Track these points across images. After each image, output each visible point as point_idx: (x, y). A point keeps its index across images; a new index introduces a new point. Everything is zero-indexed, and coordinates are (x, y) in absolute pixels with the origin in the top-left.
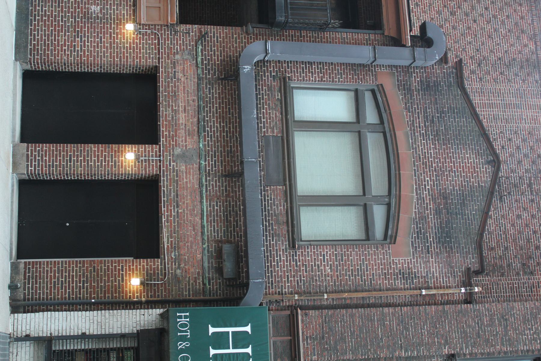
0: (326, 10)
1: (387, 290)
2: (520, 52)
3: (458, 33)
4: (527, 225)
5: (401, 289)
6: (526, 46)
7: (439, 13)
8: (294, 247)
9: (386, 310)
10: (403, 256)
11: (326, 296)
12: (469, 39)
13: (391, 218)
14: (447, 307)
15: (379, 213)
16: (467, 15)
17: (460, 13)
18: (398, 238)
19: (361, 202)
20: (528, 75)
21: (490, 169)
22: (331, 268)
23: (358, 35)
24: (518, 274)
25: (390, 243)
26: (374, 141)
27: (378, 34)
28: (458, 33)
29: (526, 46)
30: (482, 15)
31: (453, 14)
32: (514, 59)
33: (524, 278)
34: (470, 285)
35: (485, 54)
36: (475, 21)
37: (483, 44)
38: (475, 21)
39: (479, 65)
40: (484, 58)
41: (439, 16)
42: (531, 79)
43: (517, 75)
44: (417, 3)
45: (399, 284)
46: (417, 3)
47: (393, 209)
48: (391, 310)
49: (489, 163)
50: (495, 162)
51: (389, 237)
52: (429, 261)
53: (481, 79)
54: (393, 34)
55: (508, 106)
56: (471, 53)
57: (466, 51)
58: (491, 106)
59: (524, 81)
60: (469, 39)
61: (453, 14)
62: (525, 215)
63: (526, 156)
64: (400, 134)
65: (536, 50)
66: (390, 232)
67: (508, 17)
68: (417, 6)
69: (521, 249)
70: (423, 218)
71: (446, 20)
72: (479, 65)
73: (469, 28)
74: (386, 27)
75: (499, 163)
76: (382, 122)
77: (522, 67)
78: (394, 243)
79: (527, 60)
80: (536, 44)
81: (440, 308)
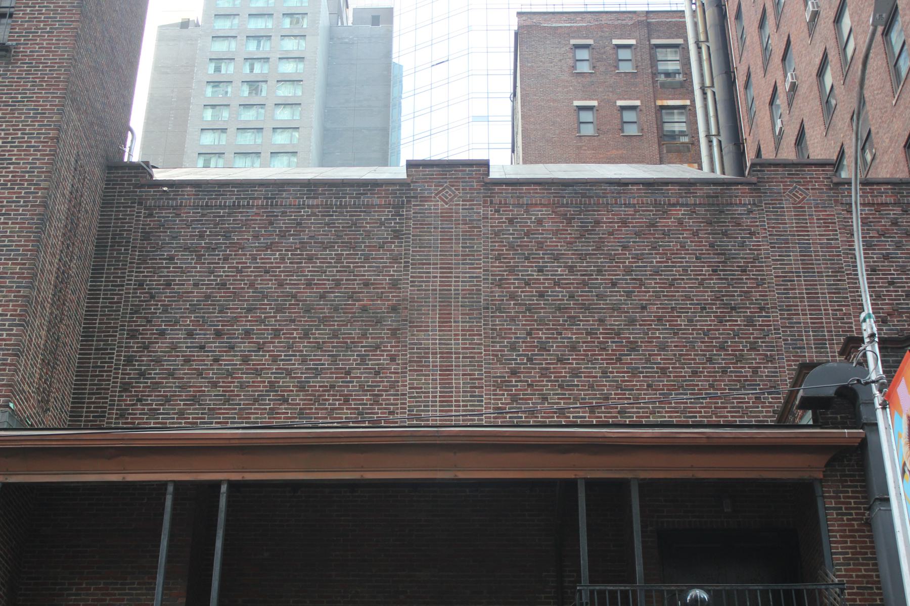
0: (799, 593)
2: (695, 234)
3: (672, 341)
6: (680, 222)
7: (634, 372)
12: (682, 322)
16: (632, 322)
17: (630, 334)
20: (739, 224)
23: (833, 531)
27: (823, 492)
28: (672, 341)
29: (680, 222)
30: (629, 294)
31: (633, 347)
32: (712, 245)
35: (708, 296)
36: (644, 308)
37: (688, 298)
38: (644, 308)
40: (717, 298)
41: (642, 372)
42: (746, 221)
43: (742, 245)
44: (619, 412)
46: (619, 412)
53: (762, 309)
54: (820, 461)
55: (808, 268)
56: (709, 321)
57: (709, 330)
58: (813, 296)
59: (752, 234)
60: (682, 322)
61: (633, 347)
65: (687, 205)
67: (625, 248)
68: (626, 413)
71: (648, 361)
73: (660, 319)
74: (806, 475)
77: (725, 234)
79: (710, 223)
80: (674, 205)
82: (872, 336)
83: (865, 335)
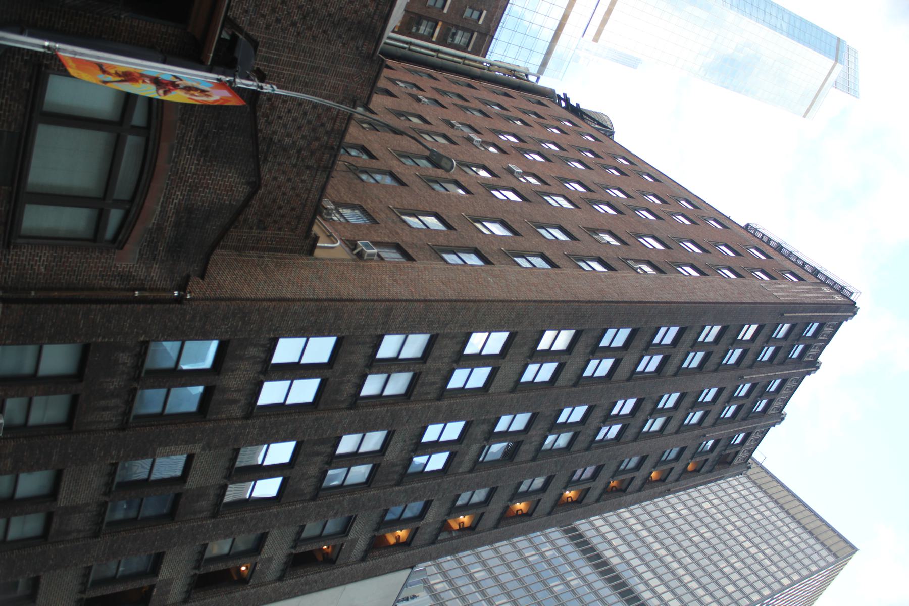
1: (102, 289)
2: (356, 12)
4: (279, 187)
5: (115, 290)
6: (366, 6)
8: (8, 247)
9: (94, 306)
10: (128, 261)
11: (33, 293)
13: (126, 225)
14: (155, 306)
15: (115, 216)
18: (127, 246)
19: (97, 203)
20: (352, 39)
21: (247, 189)
22: (46, 268)
24: (251, 228)
25: (118, 248)
26: (132, 142)
32: (346, 19)
33: (255, 232)
34: (185, 291)
39: (304, 17)
40: (314, 10)
43: (340, 37)
45: (115, 284)
47: (131, 216)
48: (99, 306)
49: (248, 183)
50: (255, 185)
51: (118, 242)
52: (152, 267)
53: (299, 34)
58: (295, 65)
59: (344, 45)
62: (282, 178)
63: (309, 122)
64: (164, 146)
65: (374, 14)
66: (120, 237)
69: (264, 207)
70: (159, 228)
72: (304, 17)
75: (259, 187)
76: (148, 127)
77: (350, 29)
78: (122, 249)
79: (359, 23)
80: (377, 6)
81: (149, 306)
82: (261, 88)
83: (263, 85)
